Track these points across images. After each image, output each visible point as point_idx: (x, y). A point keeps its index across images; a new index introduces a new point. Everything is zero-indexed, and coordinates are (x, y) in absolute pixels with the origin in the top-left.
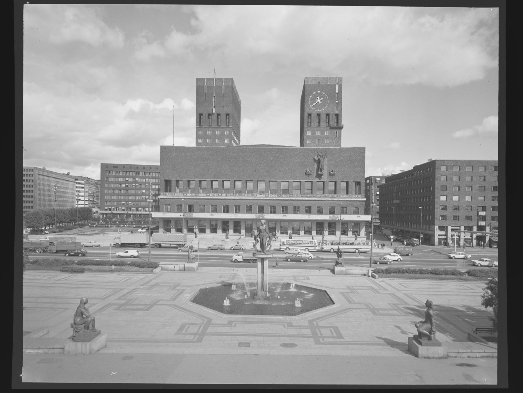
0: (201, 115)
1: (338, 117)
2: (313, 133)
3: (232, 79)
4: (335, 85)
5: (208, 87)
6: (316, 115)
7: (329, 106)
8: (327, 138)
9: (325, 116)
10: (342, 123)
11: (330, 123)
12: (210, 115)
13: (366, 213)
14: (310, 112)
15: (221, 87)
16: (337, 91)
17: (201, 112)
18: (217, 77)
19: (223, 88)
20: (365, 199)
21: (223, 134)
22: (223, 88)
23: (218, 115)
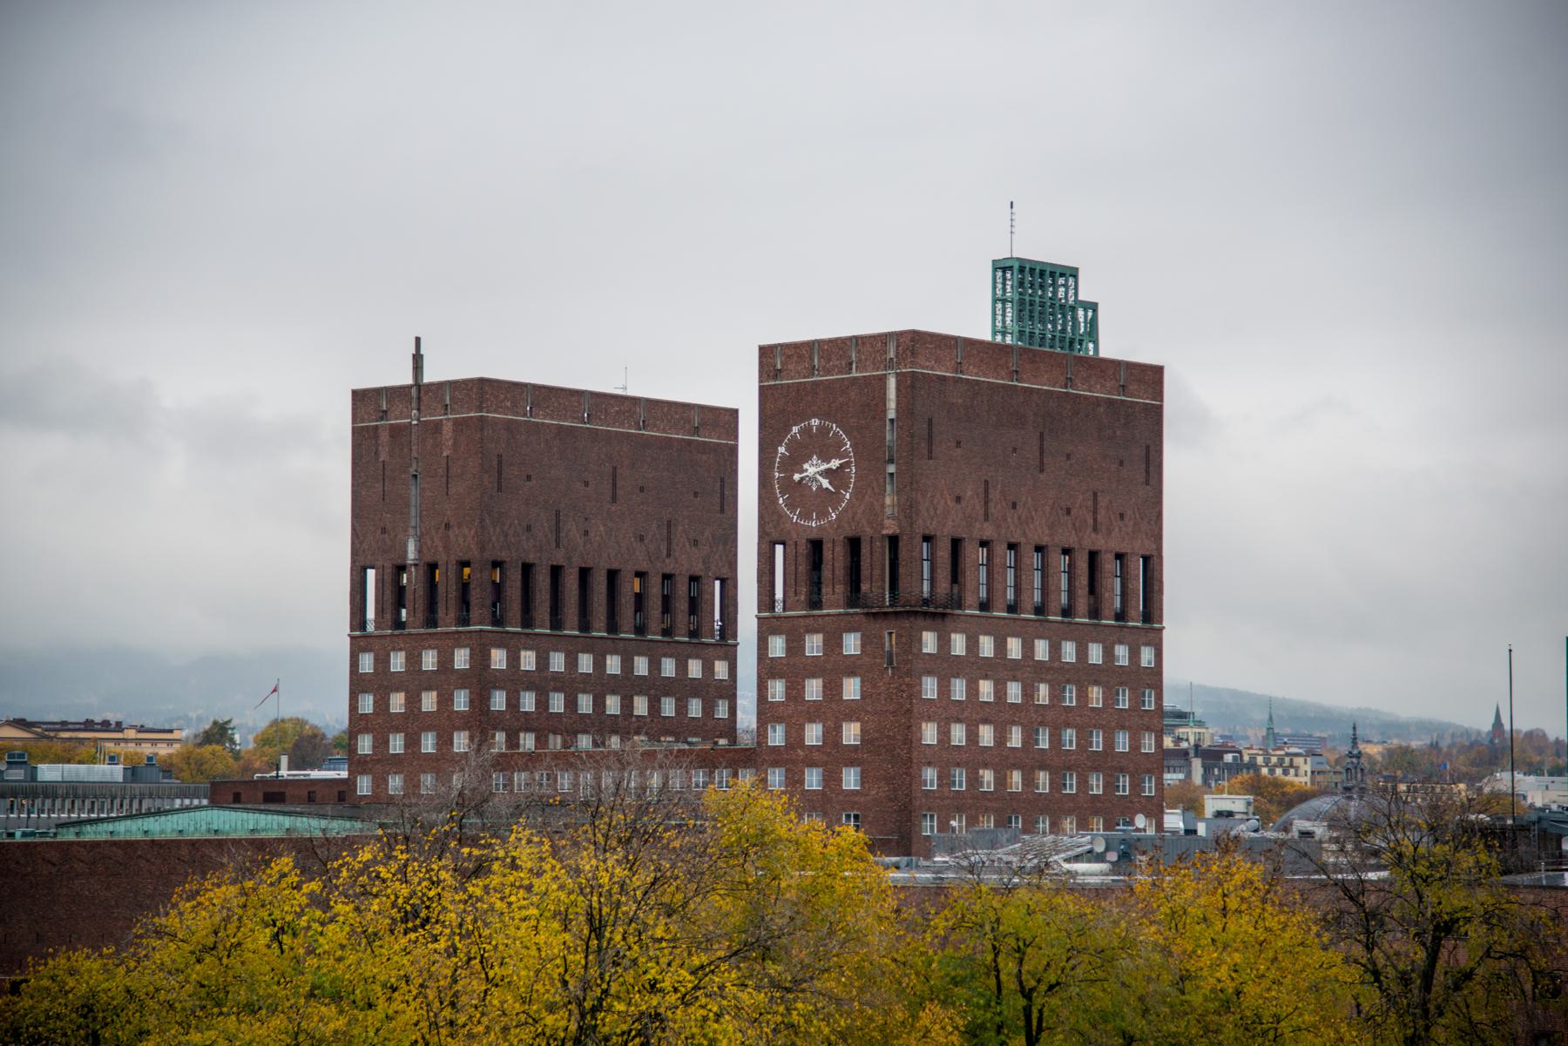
4: (882, 380)
5: (396, 431)
7: (858, 493)
11: (864, 587)
15: (437, 426)
19: (447, 430)
21: (445, 662)
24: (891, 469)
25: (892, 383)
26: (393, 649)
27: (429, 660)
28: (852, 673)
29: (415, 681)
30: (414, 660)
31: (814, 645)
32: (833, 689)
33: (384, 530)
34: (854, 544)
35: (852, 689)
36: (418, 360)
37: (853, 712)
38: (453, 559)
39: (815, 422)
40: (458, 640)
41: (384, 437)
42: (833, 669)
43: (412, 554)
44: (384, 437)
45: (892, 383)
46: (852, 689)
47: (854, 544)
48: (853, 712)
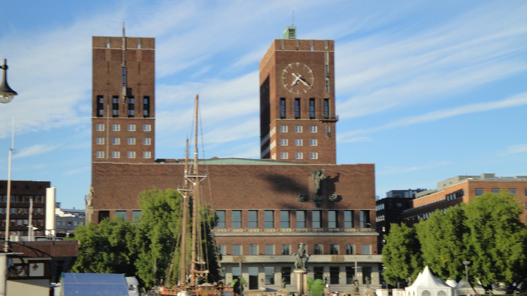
0: (99, 97)
1: (329, 102)
4: (323, 54)
5: (113, 52)
6: (293, 100)
8: (314, 137)
9: (308, 101)
12: (117, 97)
13: (379, 252)
14: (283, 96)
15: (134, 52)
16: (327, 63)
17: (101, 94)
24: (327, 79)
26: (114, 124)
27: (133, 128)
29: (125, 135)
30: (124, 128)
31: (300, 130)
32: (307, 143)
33: (108, 84)
37: (315, 149)
38: (142, 95)
39: (298, 63)
40: (145, 122)
41: (108, 54)
42: (307, 137)
43: (124, 92)
44: (108, 54)
45: (328, 55)
46: (315, 143)
48: (315, 149)
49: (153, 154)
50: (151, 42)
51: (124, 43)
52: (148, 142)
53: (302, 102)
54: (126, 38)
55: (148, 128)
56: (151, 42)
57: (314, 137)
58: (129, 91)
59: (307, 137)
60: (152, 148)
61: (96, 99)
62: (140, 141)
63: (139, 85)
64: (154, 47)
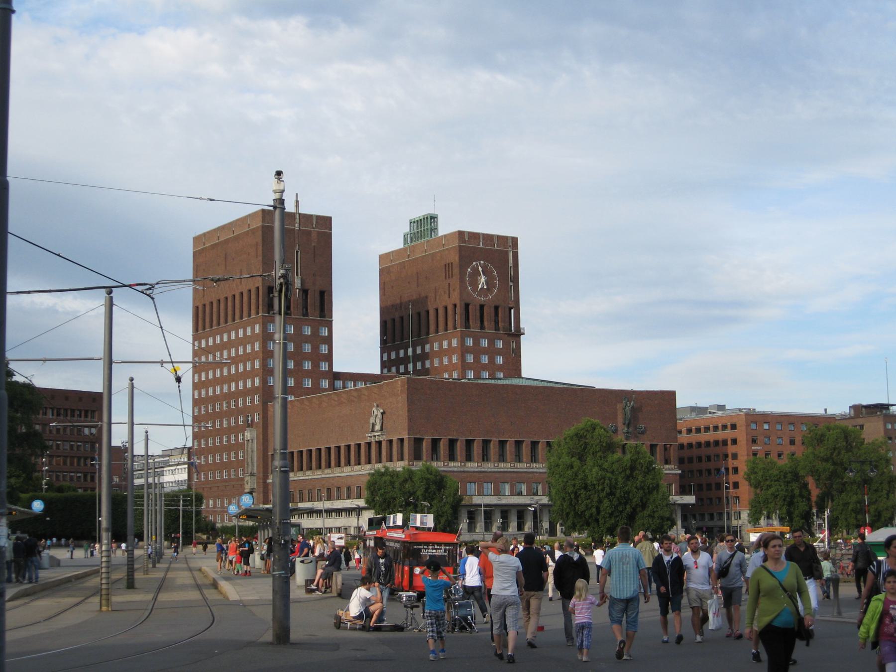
2: (476, 342)
3: (330, 219)
4: (507, 252)
8: (499, 352)
9: (493, 310)
10: (522, 326)
14: (468, 301)
15: (309, 233)
16: (511, 264)
18: (302, 210)
19: (314, 235)
20: (680, 472)
21: (315, 332)
22: (314, 235)
23: (305, 292)
24: (511, 284)
25: (511, 254)
27: (308, 331)
28: (499, 354)
29: (299, 339)
31: (485, 343)
34: (496, 308)
35: (500, 360)
36: (297, 202)
39: (482, 262)
42: (492, 352)
43: (298, 283)
45: (511, 254)
46: (500, 360)
47: (496, 308)
49: (331, 366)
50: (326, 222)
51: (297, 221)
52: (324, 349)
53: (486, 309)
54: (300, 214)
55: (325, 332)
56: (326, 222)
57: (499, 352)
58: (303, 282)
59: (492, 352)
60: (329, 358)
61: (266, 291)
62: (315, 348)
63: (314, 275)
64: (331, 229)
